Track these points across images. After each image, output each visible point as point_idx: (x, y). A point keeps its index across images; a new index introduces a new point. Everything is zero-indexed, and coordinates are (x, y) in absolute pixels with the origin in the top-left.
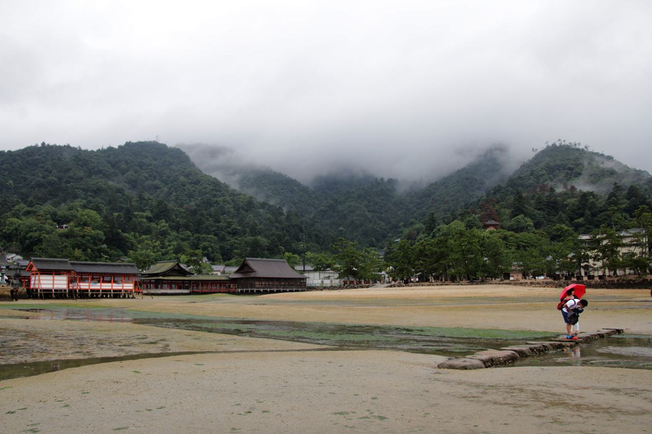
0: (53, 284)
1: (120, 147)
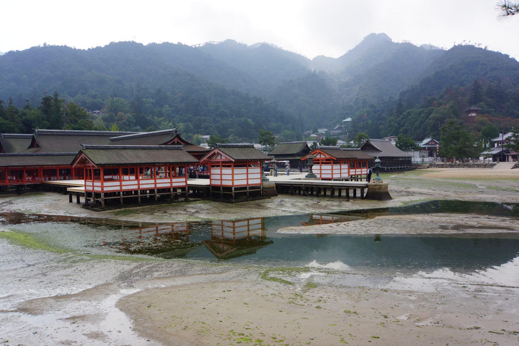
0: (332, 174)
1: (106, 46)
